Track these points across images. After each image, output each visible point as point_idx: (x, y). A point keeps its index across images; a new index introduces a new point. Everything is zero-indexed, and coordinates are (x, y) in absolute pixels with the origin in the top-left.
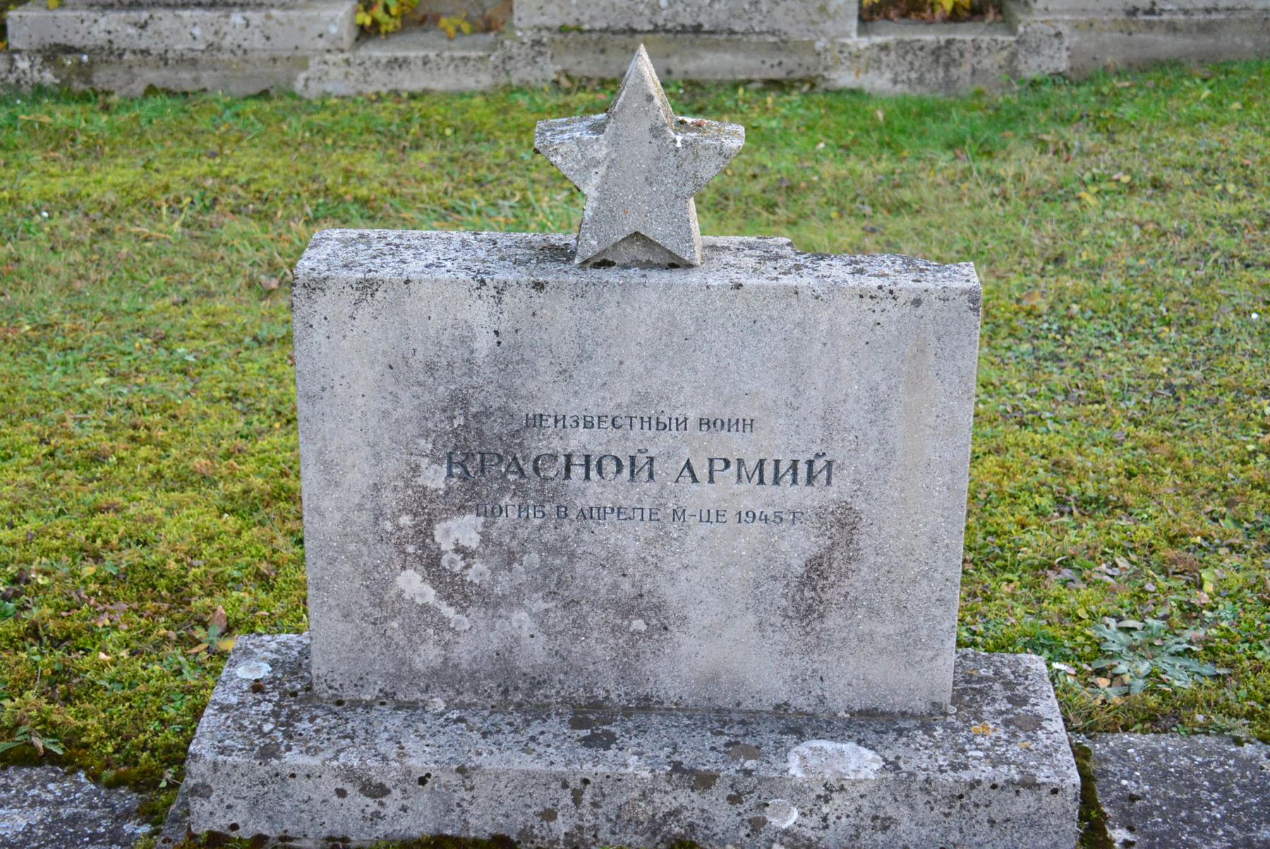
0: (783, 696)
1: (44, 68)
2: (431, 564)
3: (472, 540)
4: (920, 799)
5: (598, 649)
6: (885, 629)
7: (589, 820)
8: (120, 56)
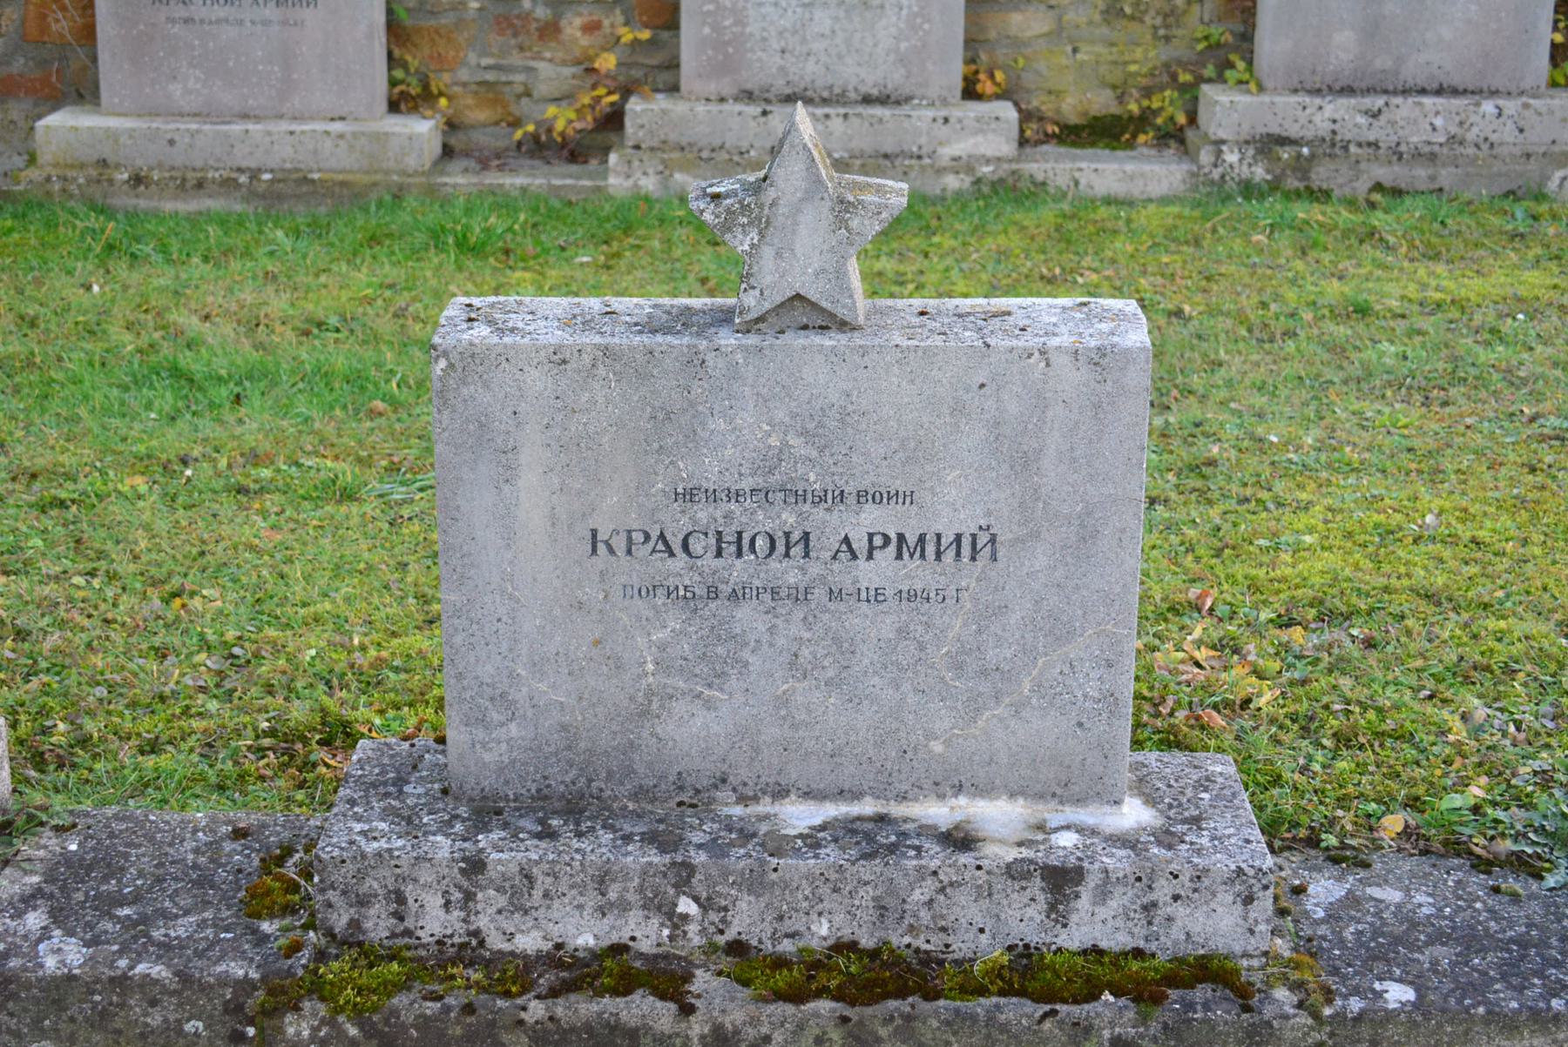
1: (1256, 162)
8: (1346, 148)
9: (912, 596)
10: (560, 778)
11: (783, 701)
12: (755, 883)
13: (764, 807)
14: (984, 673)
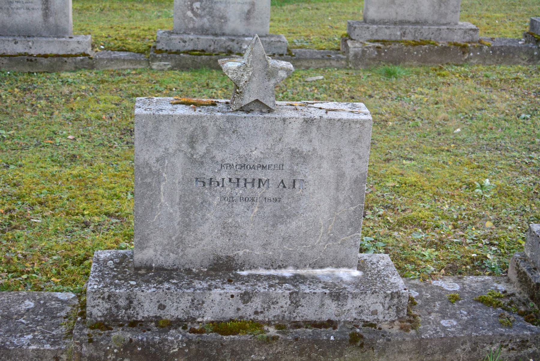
0: (244, 33)
2: (192, 10)
3: (199, 7)
5: (216, 24)
6: (259, 22)
7: (216, 47)
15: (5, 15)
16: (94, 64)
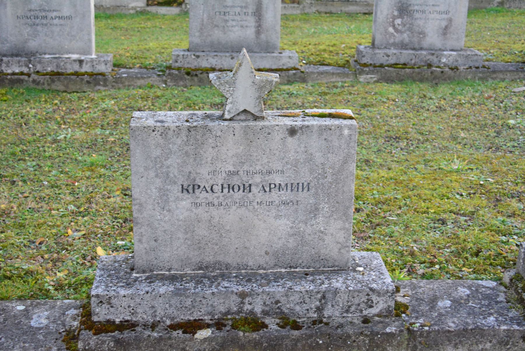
2: (394, 26)
3: (400, 23)
4: (462, 57)
5: (415, 40)
6: (455, 37)
7: (417, 61)
9: (61, 25)
10: (15, 52)
11: (45, 40)
12: (40, 62)
13: (43, 56)
14: (72, 36)
15: (220, 32)
16: (305, 77)
